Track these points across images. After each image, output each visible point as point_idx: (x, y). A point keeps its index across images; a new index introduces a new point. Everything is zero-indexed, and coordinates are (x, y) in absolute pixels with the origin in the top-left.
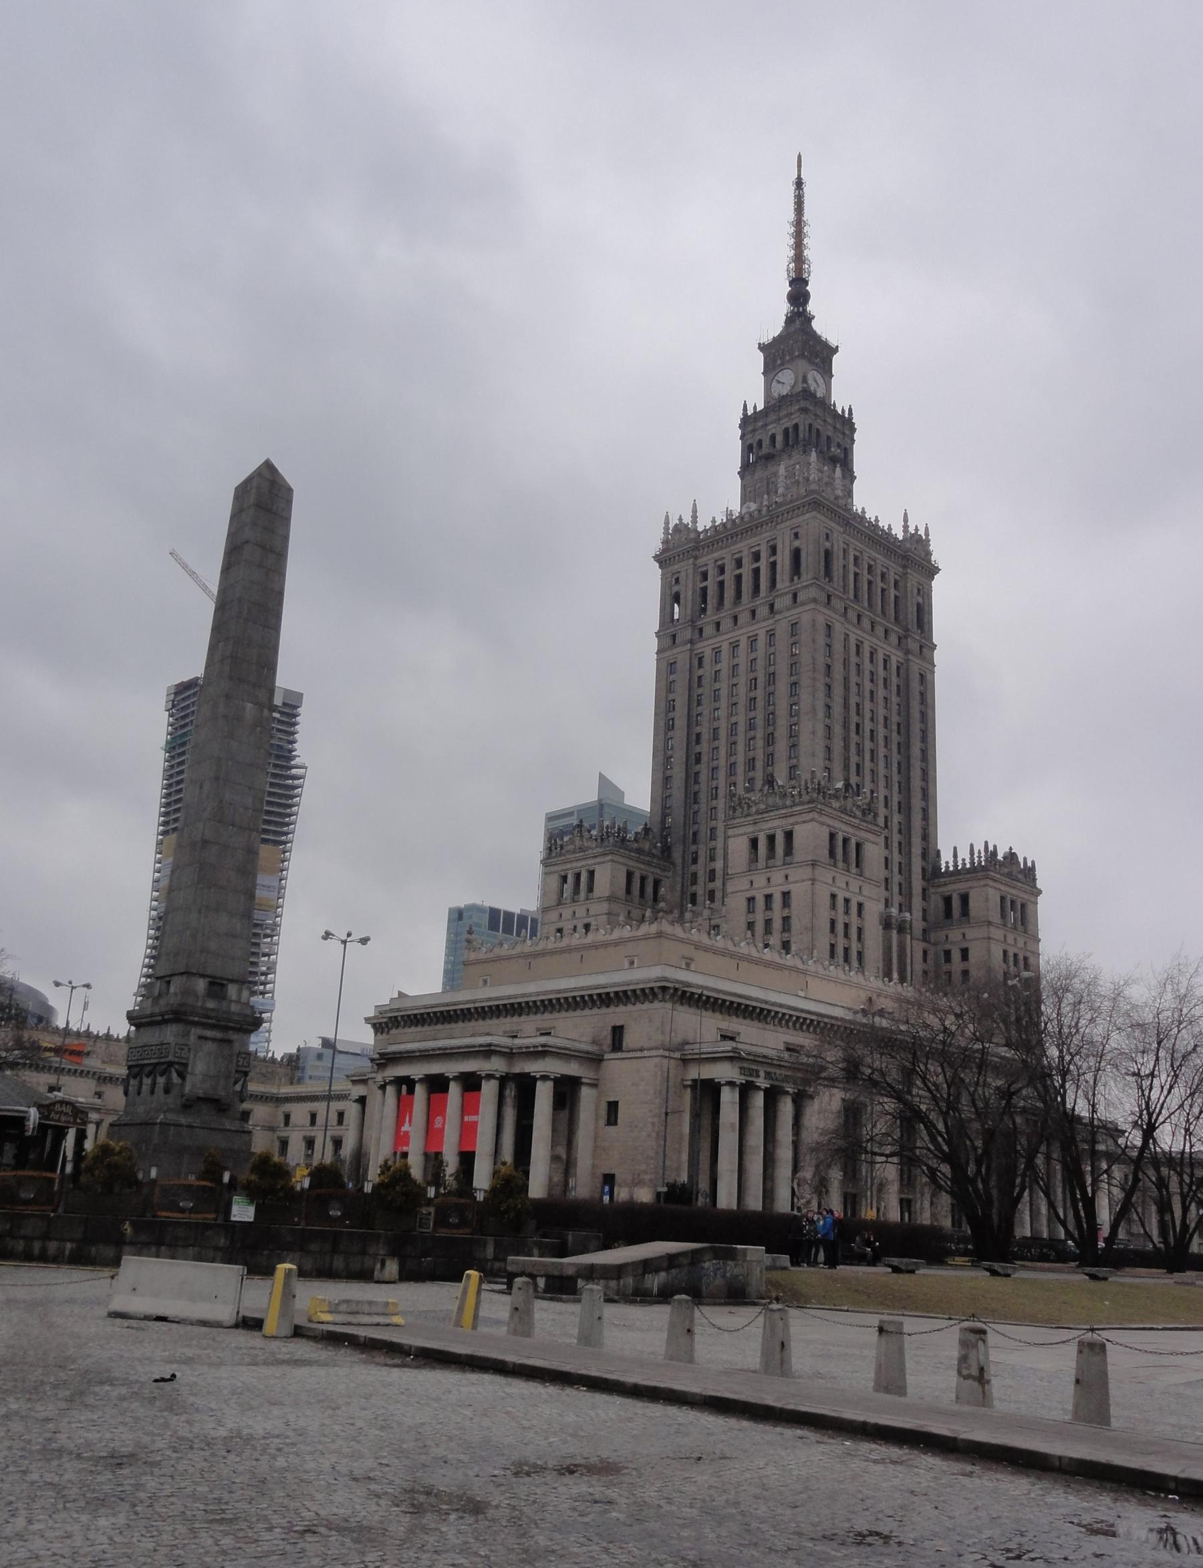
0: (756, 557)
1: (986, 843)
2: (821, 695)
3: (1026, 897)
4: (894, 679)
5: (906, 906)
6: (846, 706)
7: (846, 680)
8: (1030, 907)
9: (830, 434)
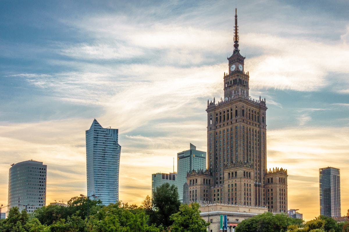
0: (228, 111)
5: (260, 181)
6: (247, 142)
8: (285, 179)
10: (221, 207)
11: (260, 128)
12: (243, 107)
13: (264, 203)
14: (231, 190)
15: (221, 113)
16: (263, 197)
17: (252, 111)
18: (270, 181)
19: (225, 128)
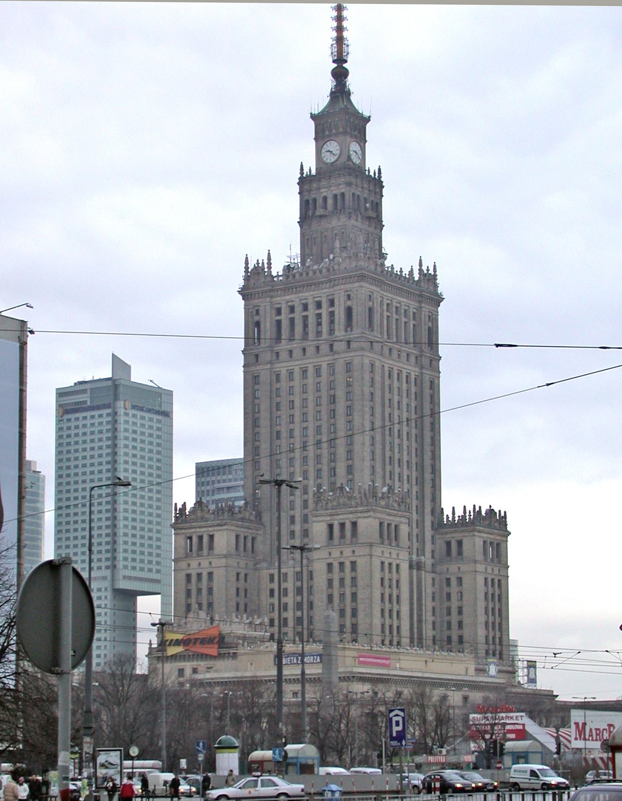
0: (319, 305)
2: (367, 416)
5: (421, 551)
8: (502, 545)
9: (366, 195)
13: (434, 623)
14: (336, 584)
15: (292, 309)
18: (452, 551)
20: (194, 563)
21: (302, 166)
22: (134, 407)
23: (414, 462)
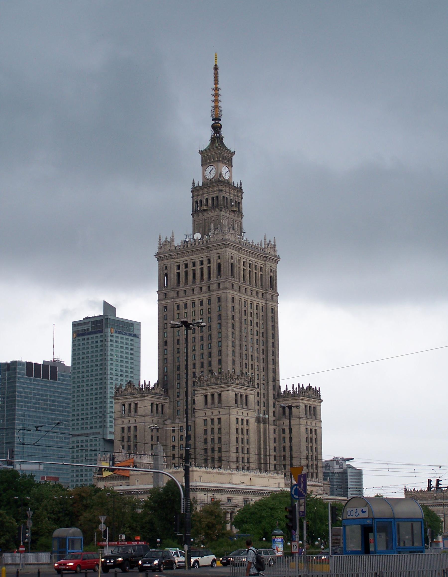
1: (299, 384)
3: (316, 404)
4: (261, 313)
5: (267, 412)
7: (240, 328)
8: (318, 408)
9: (232, 198)
10: (200, 474)
11: (266, 300)
12: (232, 259)
14: (209, 432)
15: (186, 266)
16: (272, 445)
17: (250, 264)
18: (287, 412)
19: (196, 297)
20: (126, 421)
21: (194, 181)
22: (116, 332)
23: (261, 357)
